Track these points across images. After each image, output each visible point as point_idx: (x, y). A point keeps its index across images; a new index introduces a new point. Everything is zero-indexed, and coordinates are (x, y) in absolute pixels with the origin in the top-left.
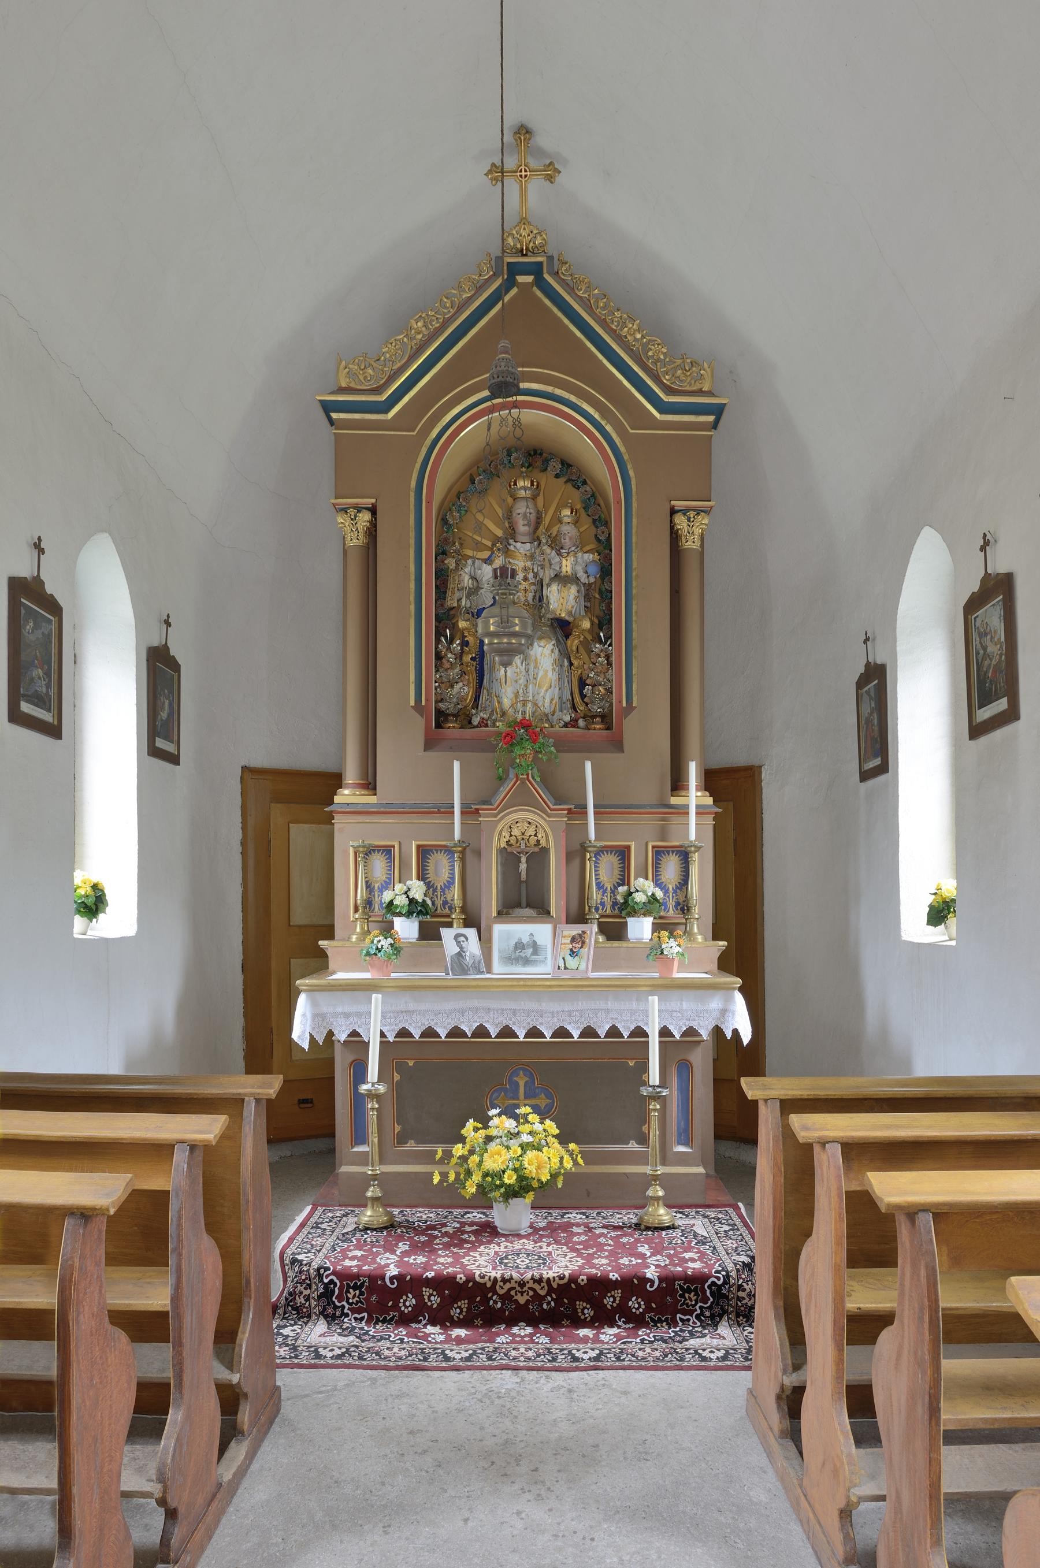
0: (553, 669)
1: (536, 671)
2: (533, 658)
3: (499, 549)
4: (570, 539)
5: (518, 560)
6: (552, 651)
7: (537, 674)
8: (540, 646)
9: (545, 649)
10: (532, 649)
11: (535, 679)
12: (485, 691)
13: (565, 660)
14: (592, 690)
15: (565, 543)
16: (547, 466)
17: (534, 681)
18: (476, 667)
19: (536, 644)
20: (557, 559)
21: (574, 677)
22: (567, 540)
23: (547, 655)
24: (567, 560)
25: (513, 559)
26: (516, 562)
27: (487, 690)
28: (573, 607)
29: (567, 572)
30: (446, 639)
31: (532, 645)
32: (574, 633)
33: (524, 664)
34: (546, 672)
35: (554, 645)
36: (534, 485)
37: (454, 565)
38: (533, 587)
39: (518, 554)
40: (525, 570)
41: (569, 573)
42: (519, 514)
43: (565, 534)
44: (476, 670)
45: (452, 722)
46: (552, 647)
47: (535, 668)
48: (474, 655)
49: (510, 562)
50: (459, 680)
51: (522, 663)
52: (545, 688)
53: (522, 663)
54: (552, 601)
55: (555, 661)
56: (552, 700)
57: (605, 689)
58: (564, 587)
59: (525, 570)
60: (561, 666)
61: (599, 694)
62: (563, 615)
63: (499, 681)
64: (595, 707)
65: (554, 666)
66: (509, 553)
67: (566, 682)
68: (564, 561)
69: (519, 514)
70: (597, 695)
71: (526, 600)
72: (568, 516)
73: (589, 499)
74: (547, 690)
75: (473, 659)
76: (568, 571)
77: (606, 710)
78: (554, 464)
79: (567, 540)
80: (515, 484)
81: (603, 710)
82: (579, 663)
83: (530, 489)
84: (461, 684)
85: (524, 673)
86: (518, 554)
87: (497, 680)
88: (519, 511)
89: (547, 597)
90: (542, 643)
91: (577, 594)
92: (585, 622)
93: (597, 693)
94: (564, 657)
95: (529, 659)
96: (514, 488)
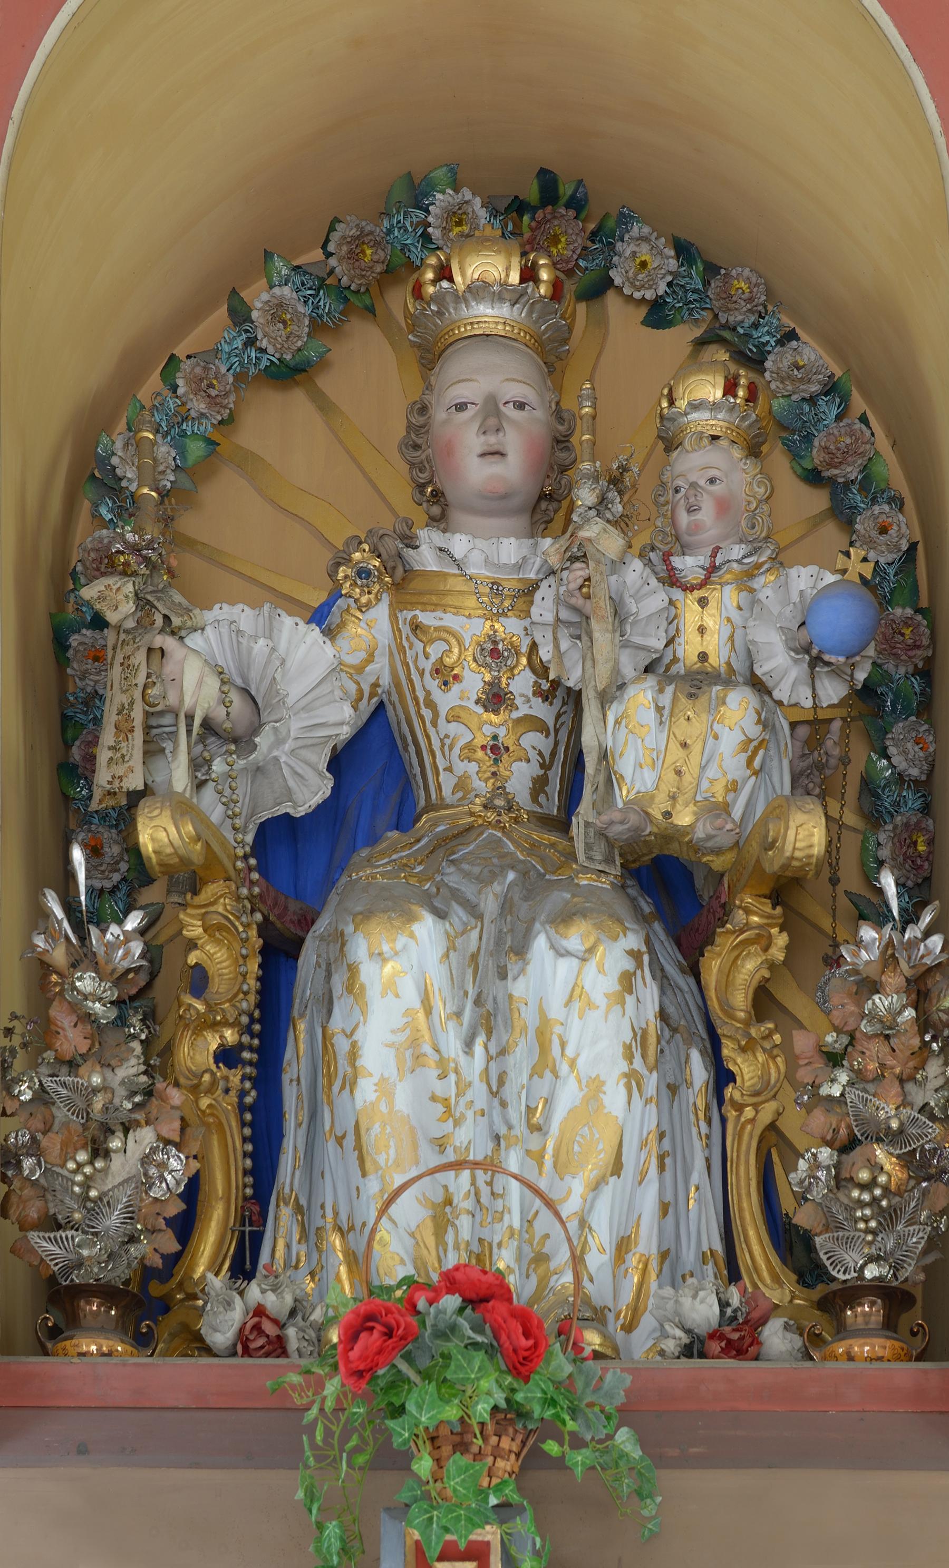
0: (632, 1080)
1: (543, 1086)
2: (529, 1016)
3: (363, 573)
4: (723, 506)
5: (458, 610)
6: (627, 982)
7: (548, 1102)
8: (562, 953)
9: (591, 968)
10: (522, 971)
11: (537, 1128)
12: (286, 1212)
13: (696, 1057)
14: (838, 1166)
15: (696, 528)
16: (609, 266)
17: (534, 1142)
18: (242, 1094)
19: (540, 944)
20: (657, 599)
21: (739, 1136)
22: (707, 514)
23: (599, 999)
24: (703, 602)
25: (435, 607)
26: (449, 620)
27: (299, 1209)
28: (734, 787)
29: (703, 657)
30: (70, 907)
31: (521, 950)
32: (740, 915)
33: (478, 1049)
34: (595, 1087)
35: (635, 955)
36: (536, 281)
37: (129, 607)
38: (533, 740)
39: (458, 584)
40: (495, 653)
41: (713, 660)
42: (461, 407)
43: (694, 485)
44: (242, 1108)
45: (101, 1330)
46: (628, 964)
47: (536, 1072)
48: (230, 1036)
49: (416, 627)
50: (139, 1116)
51: (469, 1044)
52: (590, 1172)
53: (469, 1044)
54: (625, 766)
55: (641, 1036)
56: (623, 1246)
57: (906, 1160)
58: (691, 696)
59: (495, 653)
60: (673, 1089)
61: (873, 1183)
62: (684, 818)
63: (350, 1141)
64: (853, 1258)
65: (638, 1063)
66: (416, 585)
67: (699, 1164)
68: (690, 605)
69: (461, 407)
70: (864, 1187)
71: (500, 790)
72: (714, 407)
73: (812, 400)
74: (597, 1186)
75: (226, 1056)
76: (711, 650)
77: (908, 1271)
78: (644, 254)
79: (707, 514)
80: (444, 273)
81: (896, 1268)
82: (765, 1068)
83: (517, 298)
84: (145, 1137)
85: (479, 1093)
86: (458, 584)
87: (340, 1140)
88: (462, 392)
89: (604, 755)
90: (575, 939)
91: (754, 731)
92: (797, 818)
93: (864, 1175)
94: (689, 1043)
95: (509, 1025)
96: (438, 298)
